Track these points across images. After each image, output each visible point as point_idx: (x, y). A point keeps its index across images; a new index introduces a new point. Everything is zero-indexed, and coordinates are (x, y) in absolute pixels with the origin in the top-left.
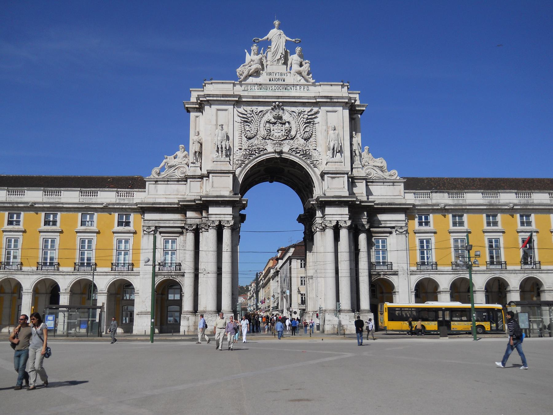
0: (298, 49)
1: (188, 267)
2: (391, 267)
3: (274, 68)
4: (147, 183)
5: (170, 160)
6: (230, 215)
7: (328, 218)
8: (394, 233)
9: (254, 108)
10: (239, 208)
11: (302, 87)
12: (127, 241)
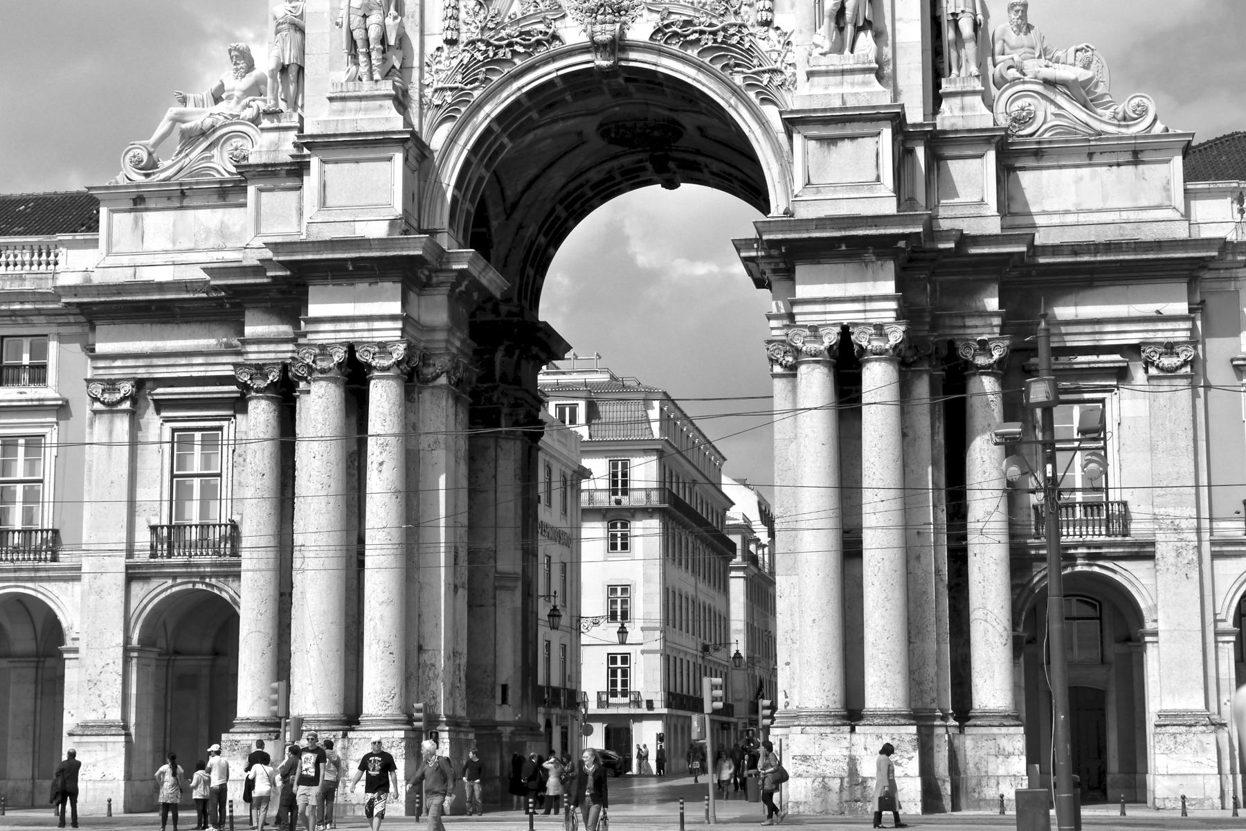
2: (1126, 526)
6: (393, 318)
7: (805, 315)
8: (1139, 375)
10: (445, 290)
12: (34, 443)
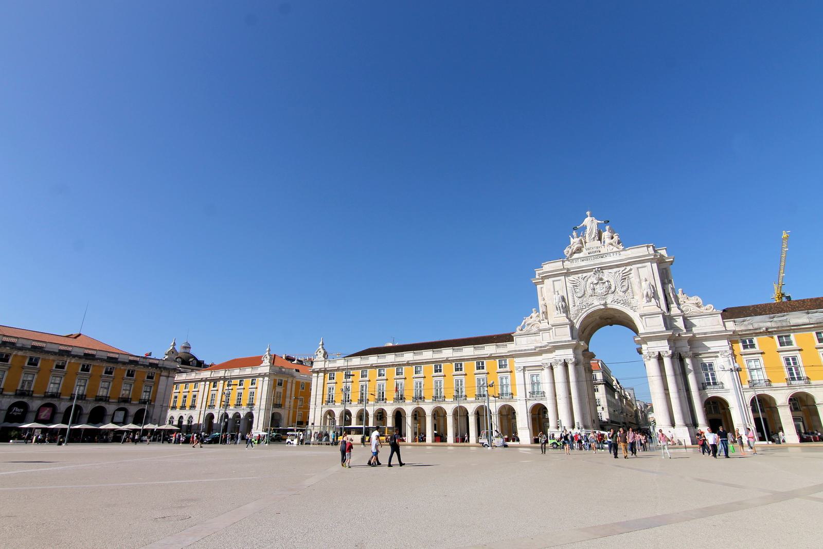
0: (607, 227)
1: (549, 394)
3: (592, 244)
4: (514, 337)
5: (528, 320)
9: (580, 275)
11: (615, 253)
12: (506, 378)
